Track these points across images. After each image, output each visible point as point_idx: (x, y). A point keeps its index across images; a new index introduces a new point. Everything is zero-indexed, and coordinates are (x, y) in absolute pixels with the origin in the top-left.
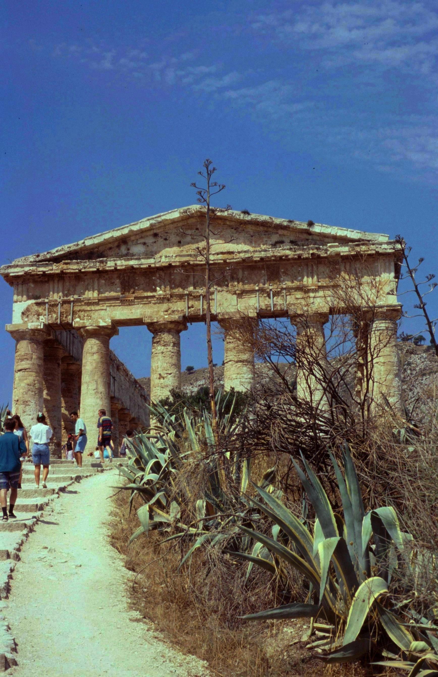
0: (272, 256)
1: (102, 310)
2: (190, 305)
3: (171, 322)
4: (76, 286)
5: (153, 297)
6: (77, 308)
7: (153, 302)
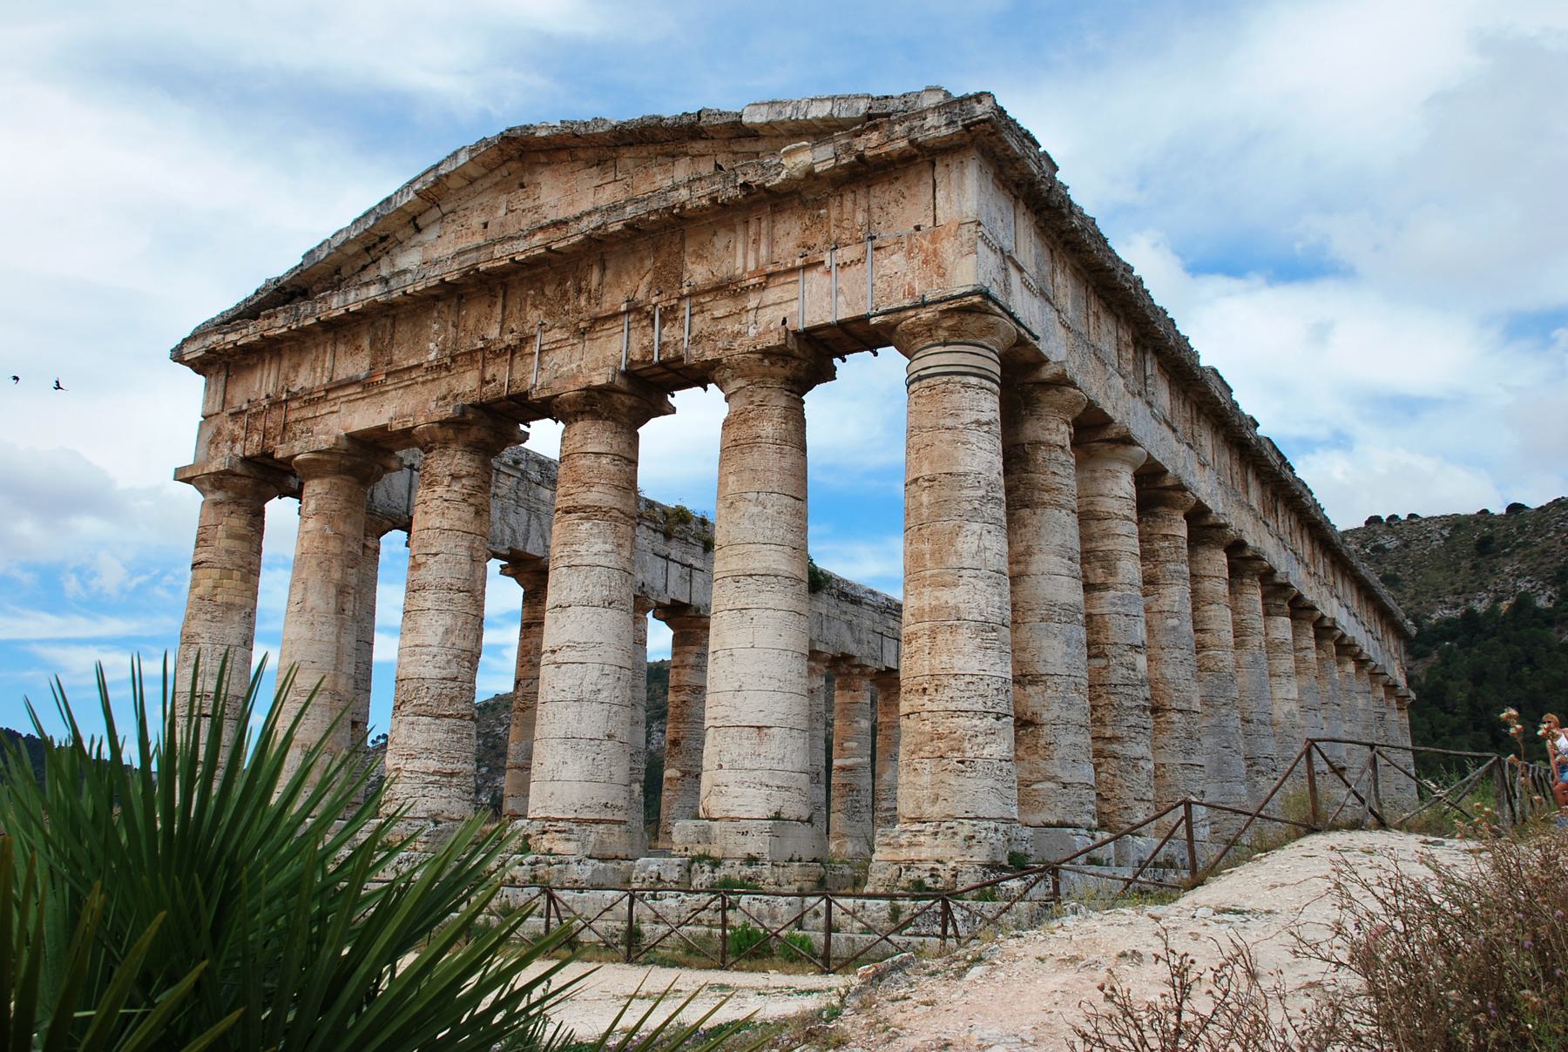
0: (649, 213)
1: (332, 412)
2: (488, 377)
3: (443, 423)
4: (299, 365)
5: (419, 366)
6: (292, 417)
7: (421, 379)
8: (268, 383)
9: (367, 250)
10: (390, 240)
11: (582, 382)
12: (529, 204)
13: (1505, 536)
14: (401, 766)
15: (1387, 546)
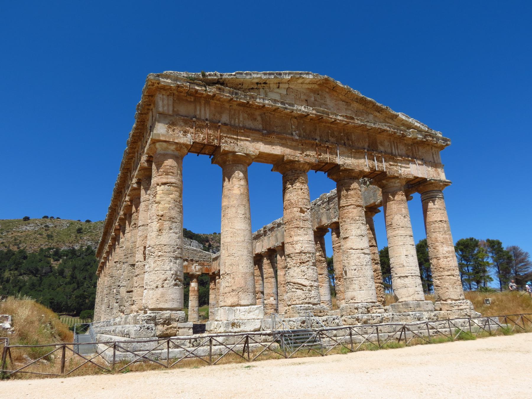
8: (205, 113)
9: (257, 83)
10: (267, 85)
11: (361, 169)
12: (323, 101)
13: (85, 229)
14: (313, 284)
15: (49, 226)
